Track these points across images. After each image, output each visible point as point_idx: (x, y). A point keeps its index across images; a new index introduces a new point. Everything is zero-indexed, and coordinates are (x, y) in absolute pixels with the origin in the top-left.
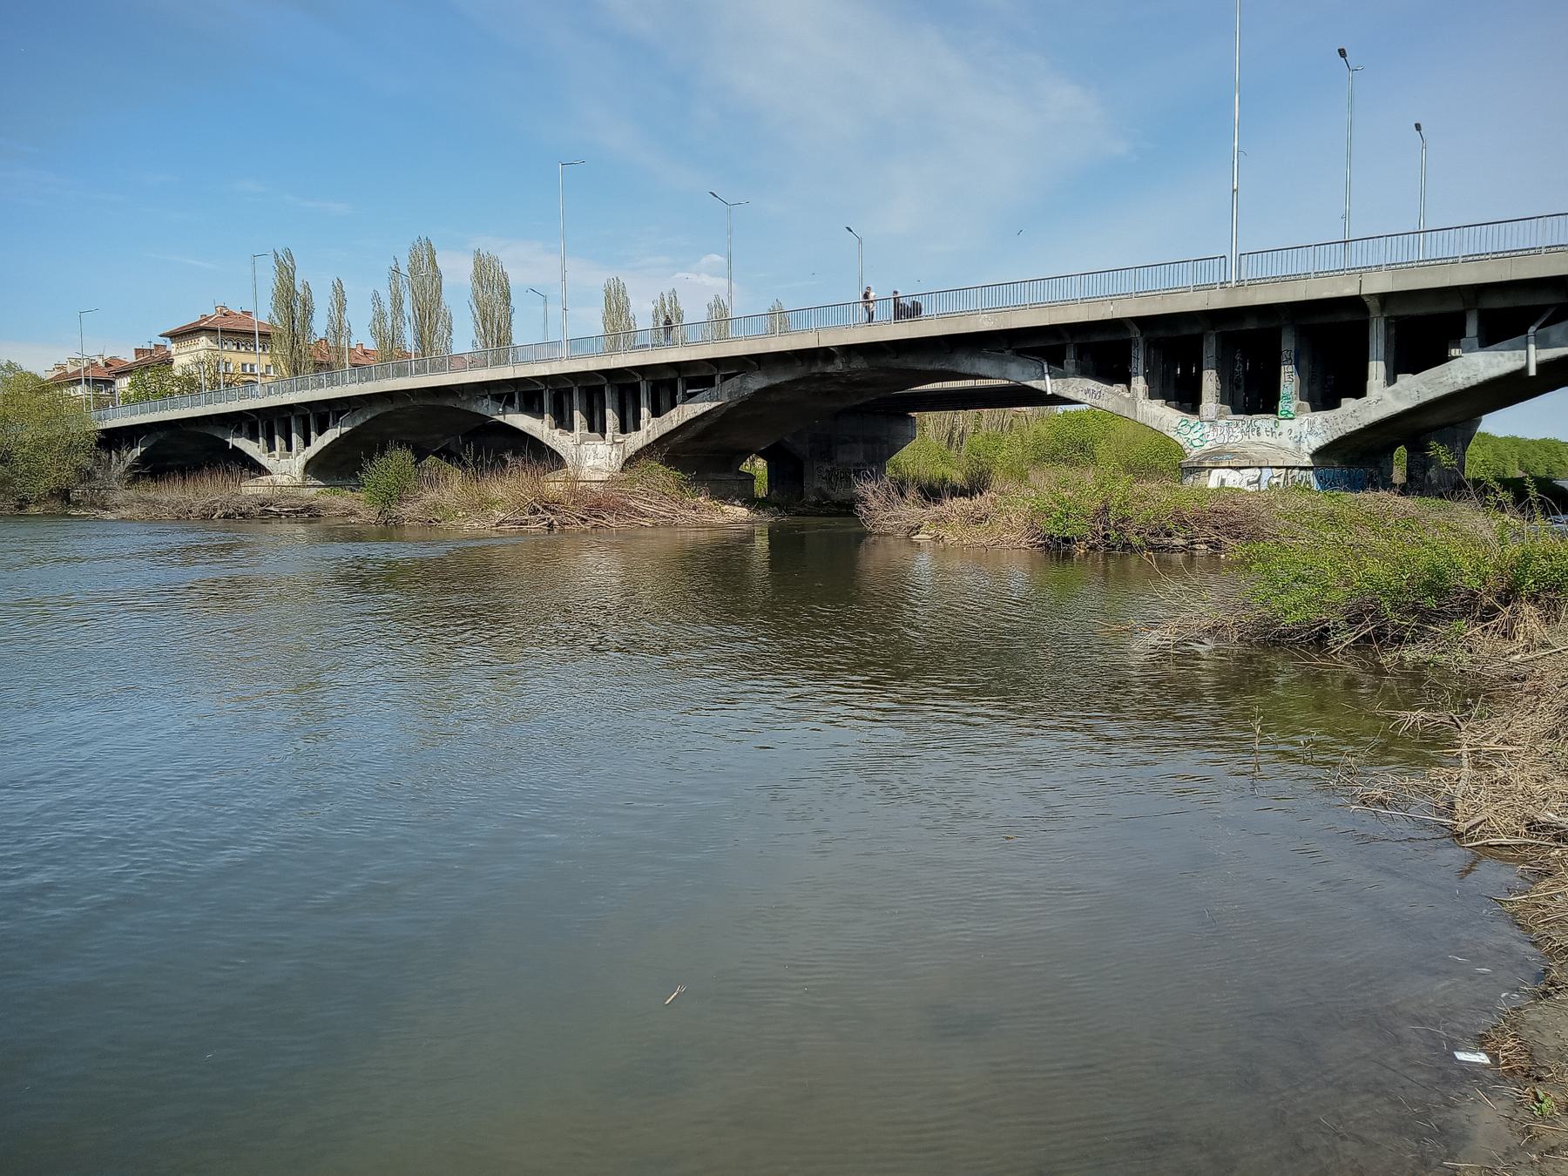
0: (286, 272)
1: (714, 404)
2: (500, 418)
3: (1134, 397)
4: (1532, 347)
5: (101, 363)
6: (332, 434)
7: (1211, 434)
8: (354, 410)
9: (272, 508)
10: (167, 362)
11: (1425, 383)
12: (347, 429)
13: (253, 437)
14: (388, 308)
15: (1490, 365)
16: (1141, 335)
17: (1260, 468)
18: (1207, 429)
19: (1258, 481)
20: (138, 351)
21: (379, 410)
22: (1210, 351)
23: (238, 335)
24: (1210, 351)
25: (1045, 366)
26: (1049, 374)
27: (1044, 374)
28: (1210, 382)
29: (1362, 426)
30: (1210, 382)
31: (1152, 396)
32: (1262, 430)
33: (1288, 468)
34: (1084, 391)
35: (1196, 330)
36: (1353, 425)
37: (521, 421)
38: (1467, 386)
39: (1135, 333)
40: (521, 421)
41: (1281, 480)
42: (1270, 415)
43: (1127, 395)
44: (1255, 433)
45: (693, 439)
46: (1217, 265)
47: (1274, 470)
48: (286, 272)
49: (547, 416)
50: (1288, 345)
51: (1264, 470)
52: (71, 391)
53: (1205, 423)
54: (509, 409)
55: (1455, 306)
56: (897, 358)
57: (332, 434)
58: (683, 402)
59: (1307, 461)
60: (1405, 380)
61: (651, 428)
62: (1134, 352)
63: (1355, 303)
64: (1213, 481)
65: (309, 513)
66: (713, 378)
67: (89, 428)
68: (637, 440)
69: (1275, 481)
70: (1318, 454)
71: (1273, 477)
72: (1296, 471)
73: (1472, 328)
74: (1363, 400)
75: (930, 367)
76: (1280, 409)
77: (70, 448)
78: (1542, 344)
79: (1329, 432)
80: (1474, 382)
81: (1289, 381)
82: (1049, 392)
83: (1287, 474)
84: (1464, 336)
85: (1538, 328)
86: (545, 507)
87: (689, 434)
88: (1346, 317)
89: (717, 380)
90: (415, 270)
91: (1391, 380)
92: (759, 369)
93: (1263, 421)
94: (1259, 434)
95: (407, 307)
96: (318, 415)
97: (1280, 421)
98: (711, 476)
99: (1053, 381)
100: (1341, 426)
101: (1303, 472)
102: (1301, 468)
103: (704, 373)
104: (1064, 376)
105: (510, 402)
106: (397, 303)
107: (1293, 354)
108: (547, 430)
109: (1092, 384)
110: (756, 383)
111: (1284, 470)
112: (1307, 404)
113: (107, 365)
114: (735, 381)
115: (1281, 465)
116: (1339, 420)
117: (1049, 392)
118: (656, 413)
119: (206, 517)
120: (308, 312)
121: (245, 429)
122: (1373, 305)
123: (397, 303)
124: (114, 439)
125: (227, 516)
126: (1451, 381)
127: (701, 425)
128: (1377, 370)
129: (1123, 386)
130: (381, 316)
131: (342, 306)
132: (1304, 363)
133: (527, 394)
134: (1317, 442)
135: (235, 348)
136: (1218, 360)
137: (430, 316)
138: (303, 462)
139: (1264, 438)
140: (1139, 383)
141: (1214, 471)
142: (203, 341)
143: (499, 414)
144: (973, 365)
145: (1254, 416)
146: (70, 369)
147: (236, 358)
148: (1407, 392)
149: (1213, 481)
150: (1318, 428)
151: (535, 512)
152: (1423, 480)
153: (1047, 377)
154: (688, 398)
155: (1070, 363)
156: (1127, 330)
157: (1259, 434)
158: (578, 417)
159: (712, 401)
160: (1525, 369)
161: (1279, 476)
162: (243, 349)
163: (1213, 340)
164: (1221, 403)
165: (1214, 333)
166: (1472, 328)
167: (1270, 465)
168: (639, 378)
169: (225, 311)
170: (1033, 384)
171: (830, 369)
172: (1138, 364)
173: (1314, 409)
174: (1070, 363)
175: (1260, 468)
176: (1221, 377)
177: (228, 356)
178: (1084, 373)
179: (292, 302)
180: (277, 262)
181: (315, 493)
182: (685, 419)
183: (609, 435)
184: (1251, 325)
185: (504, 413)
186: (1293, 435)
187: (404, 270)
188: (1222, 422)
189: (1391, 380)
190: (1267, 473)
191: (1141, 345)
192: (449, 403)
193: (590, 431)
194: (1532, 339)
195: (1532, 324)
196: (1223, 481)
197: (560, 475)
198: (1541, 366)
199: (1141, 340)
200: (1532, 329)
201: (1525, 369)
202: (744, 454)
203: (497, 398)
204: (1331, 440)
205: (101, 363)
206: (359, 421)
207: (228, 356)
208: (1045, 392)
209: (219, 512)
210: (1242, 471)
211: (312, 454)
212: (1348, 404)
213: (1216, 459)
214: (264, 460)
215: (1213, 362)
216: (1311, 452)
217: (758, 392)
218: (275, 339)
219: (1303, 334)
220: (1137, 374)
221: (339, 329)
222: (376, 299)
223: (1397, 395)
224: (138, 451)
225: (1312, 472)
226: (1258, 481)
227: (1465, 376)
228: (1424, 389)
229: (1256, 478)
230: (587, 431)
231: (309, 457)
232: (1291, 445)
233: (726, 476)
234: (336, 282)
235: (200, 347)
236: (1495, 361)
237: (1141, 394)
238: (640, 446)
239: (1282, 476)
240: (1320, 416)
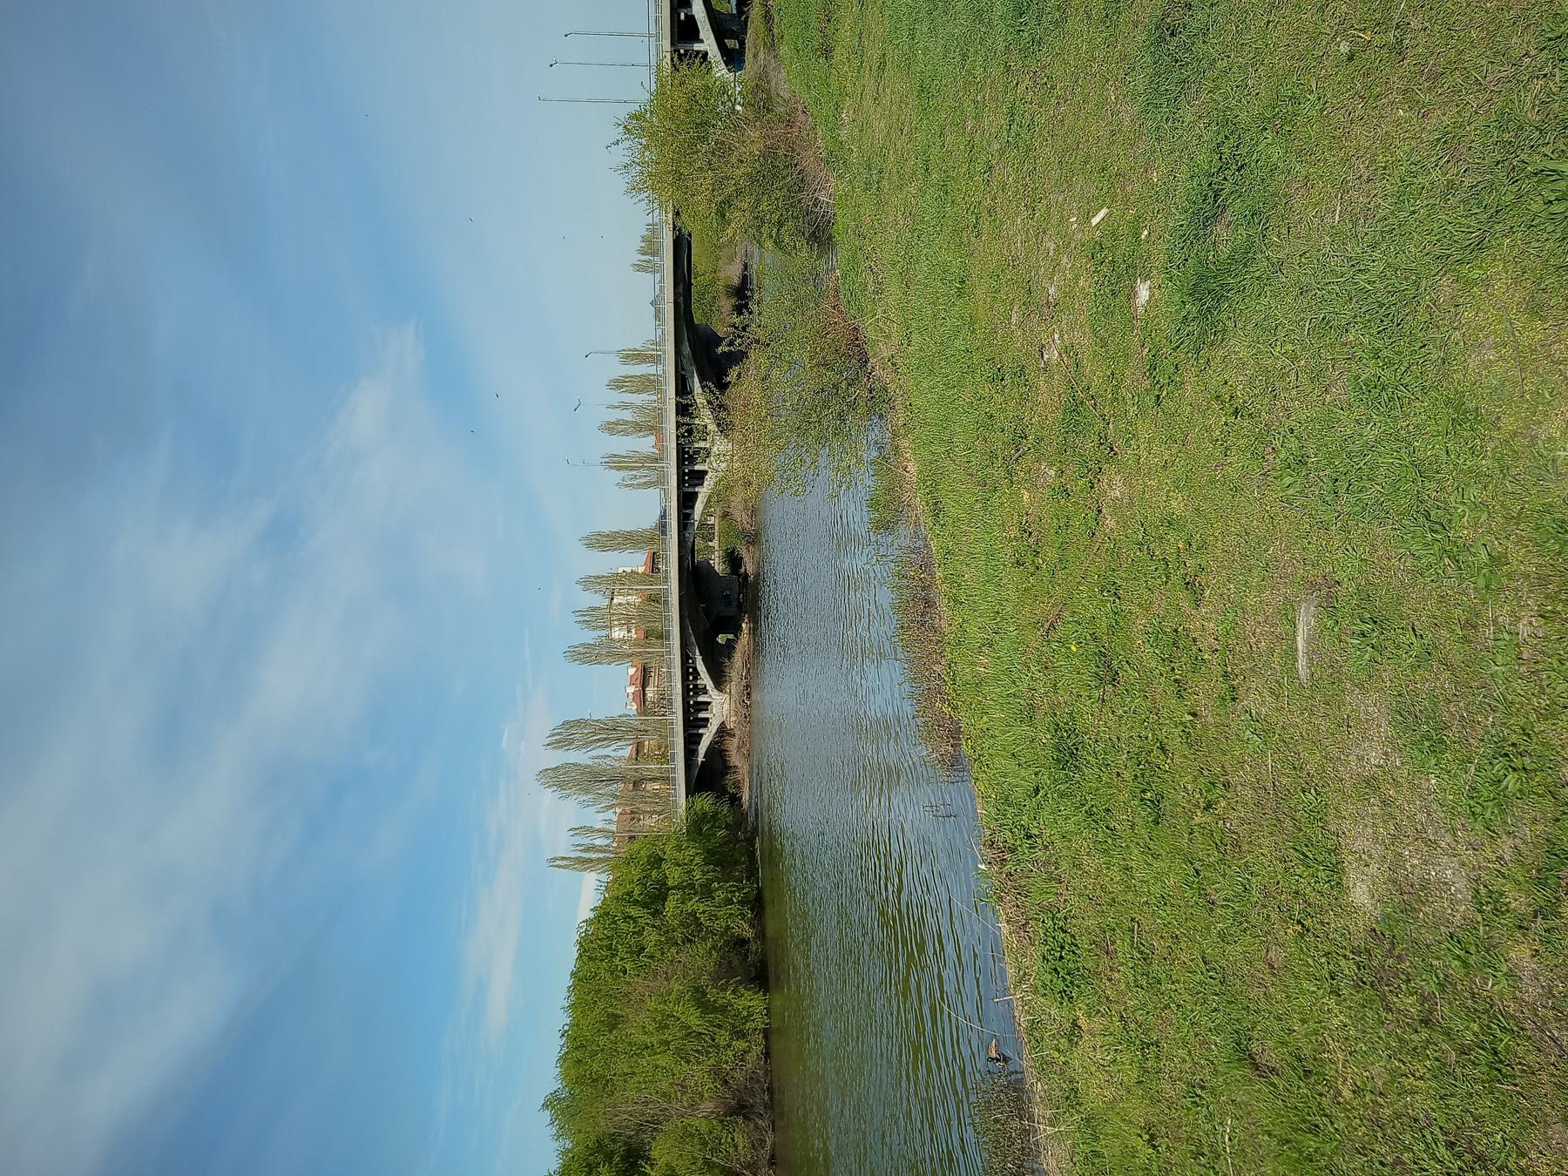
1: (696, 375)
6: (701, 667)
8: (686, 645)
12: (697, 651)
21: (688, 622)
49: (697, 490)
57: (701, 667)
60: (702, 36)
65: (748, 690)
80: (704, 10)
89: (684, 373)
91: (702, 41)
96: (688, 672)
108: (705, 490)
110: (686, 350)
128: (697, 47)
138: (716, 692)
143: (693, 523)
154: (691, 392)
159: (693, 377)
181: (734, 686)
189: (702, 41)
203: (685, 529)
211: (711, 682)
231: (713, 686)
234: (572, 833)
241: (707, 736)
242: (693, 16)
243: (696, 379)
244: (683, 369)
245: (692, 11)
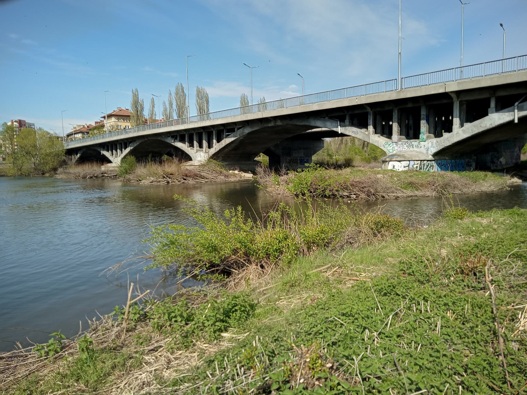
0: (136, 96)
1: (235, 138)
2: (173, 144)
3: (369, 134)
4: (516, 111)
5: (86, 127)
7: (396, 147)
9: (105, 175)
10: (103, 126)
11: (474, 126)
12: (132, 148)
13: (108, 151)
14: (168, 106)
15: (500, 119)
16: (371, 110)
17: (409, 161)
18: (394, 146)
19: (408, 166)
20: (96, 123)
22: (395, 115)
23: (125, 117)
24: (395, 115)
25: (339, 123)
26: (340, 126)
27: (338, 126)
28: (395, 127)
29: (451, 144)
30: (395, 127)
31: (376, 133)
32: (414, 146)
33: (421, 161)
34: (351, 131)
35: (391, 108)
36: (448, 144)
37: (179, 145)
38: (491, 127)
39: (369, 109)
40: (179, 145)
41: (418, 166)
42: (416, 140)
43: (367, 133)
44: (412, 147)
45: (232, 150)
46: (394, 82)
47: (415, 162)
48: (136, 96)
49: (187, 143)
50: (423, 112)
51: (411, 162)
52: (76, 136)
53: (394, 143)
54: (176, 141)
55: (485, 96)
56: (291, 120)
58: (226, 137)
59: (431, 158)
60: (467, 125)
61: (217, 146)
62: (369, 117)
63: (445, 95)
64: (390, 167)
66: (234, 129)
67: (65, 148)
68: (213, 151)
69: (415, 166)
70: (435, 155)
71: (415, 164)
72: (425, 162)
73: (493, 104)
74: (451, 133)
75: (301, 124)
76: (420, 137)
77: (57, 155)
78: (520, 109)
79: (438, 146)
80: (494, 126)
81: (424, 126)
82: (340, 132)
83: (421, 163)
84: (489, 107)
85: (519, 103)
86: (167, 176)
87: (230, 148)
88: (445, 101)
90: (177, 94)
91: (462, 125)
92: (248, 125)
93: (415, 142)
94: (413, 147)
95: (174, 106)
97: (421, 142)
98: (243, 162)
99: (341, 128)
100: (443, 144)
101: (429, 162)
102: (428, 161)
103: (232, 127)
104: (345, 126)
105: (176, 139)
106: (171, 104)
107: (425, 116)
109: (355, 129)
110: (247, 130)
111: (419, 162)
112: (432, 135)
113: (88, 127)
114: (241, 130)
115: (418, 159)
116: (442, 141)
117: (340, 132)
118: (219, 141)
119: (84, 177)
120: (142, 109)
121: (106, 148)
122: (454, 96)
123: (171, 104)
124: (71, 152)
125: (91, 178)
126: (485, 126)
127: (233, 145)
128: (456, 121)
129: (366, 129)
130: (165, 110)
131: (153, 106)
132: (431, 120)
133: (180, 135)
134: (434, 150)
135: (123, 121)
136: (398, 119)
137: (182, 109)
139: (415, 149)
140: (371, 128)
141: (390, 162)
142: (113, 119)
144: (315, 123)
145: (412, 140)
146: (78, 129)
147: (123, 124)
148: (468, 130)
149: (390, 167)
150: (434, 145)
151: (164, 177)
152: (497, 163)
153: (339, 127)
154: (227, 136)
155: (347, 122)
156: (366, 109)
157: (413, 147)
158: (195, 143)
159: (234, 137)
160: (513, 120)
161: (417, 164)
162: (125, 121)
163: (396, 111)
164: (400, 135)
165: (396, 109)
166: (493, 104)
167: (413, 159)
168: (212, 130)
169: (120, 109)
170: (335, 129)
171: (270, 125)
172: (370, 121)
173: (436, 136)
174: (347, 122)
175: (409, 161)
176: (400, 125)
177: (119, 124)
178: (352, 124)
179: (137, 104)
180: (133, 93)
182: (226, 144)
183: (204, 149)
184: (410, 105)
185: (174, 142)
186: (425, 148)
187: (173, 95)
188: (400, 143)
189: (462, 125)
190: (412, 163)
191: (371, 114)
192: (159, 138)
193: (200, 148)
194: (516, 107)
195: (517, 101)
196: (394, 166)
197: (190, 163)
198: (520, 119)
199: (371, 112)
200: (516, 104)
201: (513, 120)
202: (257, 154)
204: (439, 149)
205: (86, 127)
206: (135, 145)
207: (119, 124)
208: (338, 132)
209: (88, 176)
210: (401, 162)
212: (446, 135)
213: (392, 158)
214: (111, 158)
215: (396, 120)
216: (432, 154)
217: (249, 134)
218: (132, 117)
219: (429, 108)
220: (370, 125)
221: (152, 113)
222: (164, 103)
223: (464, 131)
224: (79, 155)
225: (434, 162)
226: (408, 166)
227: (490, 123)
228: (474, 129)
229: (407, 165)
230: (198, 148)
232: (425, 152)
233: (249, 162)
235: (112, 121)
236: (502, 117)
237: (371, 133)
238: (213, 153)
239: (419, 164)
240: (435, 140)
241: (107, 154)
242: (487, 115)
243: (233, 139)
244: (239, 129)
245: (492, 113)
